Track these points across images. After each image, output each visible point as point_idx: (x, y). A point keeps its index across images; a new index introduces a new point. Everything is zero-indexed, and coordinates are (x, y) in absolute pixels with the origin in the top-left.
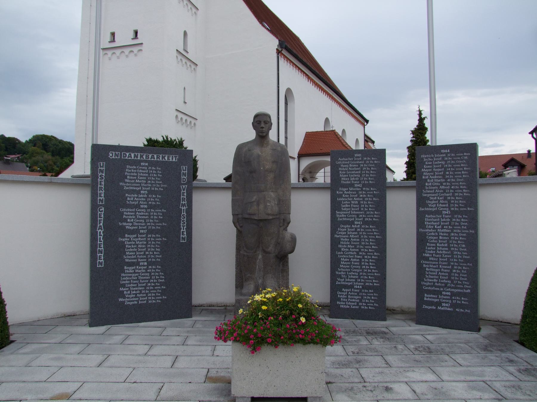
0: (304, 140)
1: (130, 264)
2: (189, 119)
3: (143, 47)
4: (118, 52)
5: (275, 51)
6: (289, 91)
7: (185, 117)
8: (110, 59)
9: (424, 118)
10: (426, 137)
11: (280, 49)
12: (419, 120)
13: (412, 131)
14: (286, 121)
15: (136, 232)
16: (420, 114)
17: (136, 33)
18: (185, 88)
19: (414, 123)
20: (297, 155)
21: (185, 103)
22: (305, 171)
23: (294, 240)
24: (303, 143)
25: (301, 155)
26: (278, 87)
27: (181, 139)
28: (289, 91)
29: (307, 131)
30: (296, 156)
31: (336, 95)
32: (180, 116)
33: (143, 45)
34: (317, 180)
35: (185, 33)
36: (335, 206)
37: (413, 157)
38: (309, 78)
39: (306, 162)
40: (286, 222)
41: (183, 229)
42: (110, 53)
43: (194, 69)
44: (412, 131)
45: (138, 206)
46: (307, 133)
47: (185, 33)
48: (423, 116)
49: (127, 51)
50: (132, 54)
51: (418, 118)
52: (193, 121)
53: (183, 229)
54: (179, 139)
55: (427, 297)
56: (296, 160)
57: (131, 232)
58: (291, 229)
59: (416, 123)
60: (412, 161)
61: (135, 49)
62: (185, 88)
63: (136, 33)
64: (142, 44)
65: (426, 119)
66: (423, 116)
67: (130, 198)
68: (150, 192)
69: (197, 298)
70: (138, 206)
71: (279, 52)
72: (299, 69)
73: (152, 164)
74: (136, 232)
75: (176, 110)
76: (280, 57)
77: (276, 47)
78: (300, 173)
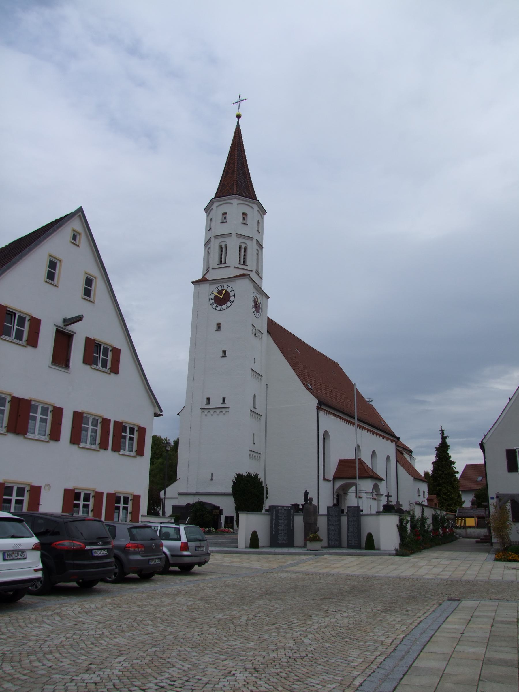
0: (338, 466)
1: (280, 533)
2: (257, 455)
3: (230, 410)
4: (212, 411)
5: (316, 407)
6: (326, 434)
7: (254, 454)
8: (206, 415)
9: (446, 437)
10: (449, 454)
11: (319, 406)
12: (442, 439)
13: (436, 448)
14: (324, 453)
15: (281, 526)
16: (443, 434)
17: (224, 399)
18: (254, 434)
19: (438, 441)
20: (332, 478)
21: (254, 444)
22: (339, 489)
23: (318, 528)
24: (337, 468)
25: (335, 478)
26: (318, 433)
27: (257, 473)
28: (326, 434)
29: (340, 459)
30: (331, 478)
31: (365, 424)
32: (252, 453)
33: (229, 408)
34: (349, 495)
35: (255, 395)
36: (328, 520)
37: (436, 472)
38: (341, 418)
39: (339, 483)
40: (316, 524)
41: (292, 526)
42: (206, 411)
43: (260, 419)
44: (436, 448)
45: (282, 520)
46: (340, 460)
47: (255, 395)
48: (445, 435)
49: (218, 411)
50: (221, 414)
51: (440, 437)
52: (259, 455)
53: (292, 526)
54: (256, 473)
55: (349, 542)
56: (332, 482)
57: (280, 526)
58: (318, 526)
59: (440, 441)
60: (436, 475)
61: (224, 411)
62: (254, 434)
63: (224, 399)
64: (229, 407)
65: (448, 437)
66: (445, 435)
67: (280, 518)
68: (284, 516)
69: (294, 545)
70: (282, 520)
71: (318, 408)
72: (333, 414)
73: (285, 510)
74: (281, 526)
75: (250, 450)
76: (319, 411)
77: (317, 405)
78: (335, 491)
